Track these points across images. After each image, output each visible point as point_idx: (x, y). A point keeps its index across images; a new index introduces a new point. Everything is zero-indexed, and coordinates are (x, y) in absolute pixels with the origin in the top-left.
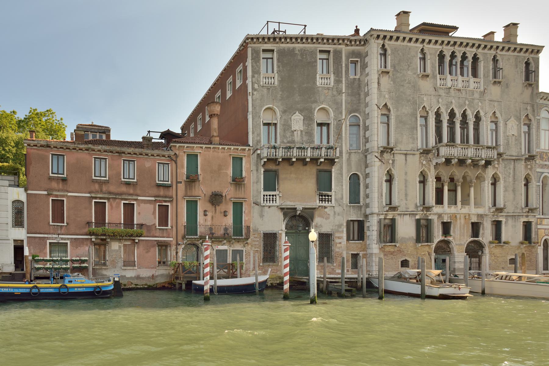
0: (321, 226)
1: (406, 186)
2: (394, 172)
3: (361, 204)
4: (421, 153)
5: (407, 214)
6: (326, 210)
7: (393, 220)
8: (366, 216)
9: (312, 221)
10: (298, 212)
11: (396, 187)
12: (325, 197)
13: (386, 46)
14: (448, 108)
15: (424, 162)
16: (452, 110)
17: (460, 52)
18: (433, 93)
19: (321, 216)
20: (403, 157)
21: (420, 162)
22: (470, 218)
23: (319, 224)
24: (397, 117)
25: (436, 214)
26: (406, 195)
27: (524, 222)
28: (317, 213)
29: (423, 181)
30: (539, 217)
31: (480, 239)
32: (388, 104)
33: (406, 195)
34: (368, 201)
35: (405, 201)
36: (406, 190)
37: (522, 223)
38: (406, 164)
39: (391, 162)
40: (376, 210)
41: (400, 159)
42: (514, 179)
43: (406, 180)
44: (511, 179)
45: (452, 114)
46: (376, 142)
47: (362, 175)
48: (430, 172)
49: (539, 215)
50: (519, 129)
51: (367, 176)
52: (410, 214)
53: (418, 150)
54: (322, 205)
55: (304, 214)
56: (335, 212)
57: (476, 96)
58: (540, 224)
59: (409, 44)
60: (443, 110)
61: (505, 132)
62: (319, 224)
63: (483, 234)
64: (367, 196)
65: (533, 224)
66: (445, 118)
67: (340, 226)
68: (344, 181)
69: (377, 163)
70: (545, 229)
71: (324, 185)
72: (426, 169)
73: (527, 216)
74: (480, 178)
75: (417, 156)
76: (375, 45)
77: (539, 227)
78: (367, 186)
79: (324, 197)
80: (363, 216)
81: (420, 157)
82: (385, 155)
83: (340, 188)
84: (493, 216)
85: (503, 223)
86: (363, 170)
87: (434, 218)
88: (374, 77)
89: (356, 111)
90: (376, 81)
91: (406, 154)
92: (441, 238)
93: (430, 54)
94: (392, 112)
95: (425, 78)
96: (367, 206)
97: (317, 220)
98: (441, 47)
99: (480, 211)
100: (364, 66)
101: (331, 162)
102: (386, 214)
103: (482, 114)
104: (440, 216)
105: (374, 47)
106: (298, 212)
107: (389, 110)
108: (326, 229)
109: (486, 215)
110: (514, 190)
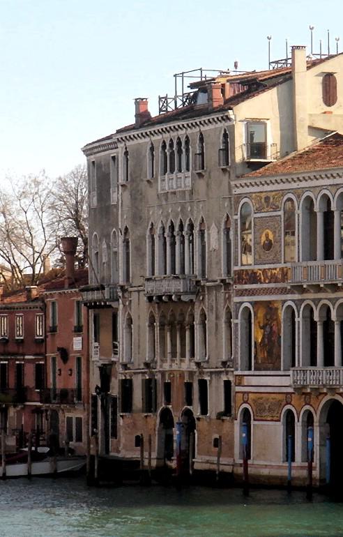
5: (140, 373)
20: (137, 293)
25: (160, 371)
27: (225, 381)
30: (236, 373)
35: (137, 355)
36: (139, 340)
37: (223, 384)
41: (134, 296)
42: (217, 318)
43: (139, 326)
44: (214, 316)
49: (237, 370)
58: (239, 385)
61: (209, 248)
70: (244, 393)
73: (227, 373)
77: (238, 389)
104: (163, 373)
109: (195, 372)
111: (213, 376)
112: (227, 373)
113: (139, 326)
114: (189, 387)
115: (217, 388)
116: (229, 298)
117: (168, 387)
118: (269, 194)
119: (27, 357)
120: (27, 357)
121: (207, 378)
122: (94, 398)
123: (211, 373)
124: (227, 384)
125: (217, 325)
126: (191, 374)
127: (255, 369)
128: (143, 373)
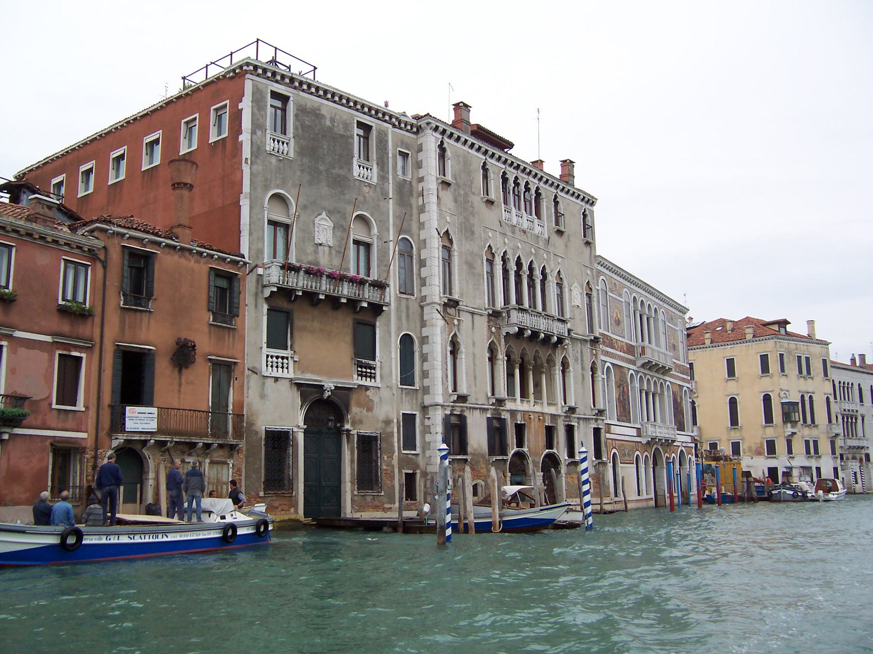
0: (361, 422)
1: (474, 364)
2: (461, 339)
3: (417, 387)
4: (489, 315)
6: (368, 393)
7: (462, 418)
8: (425, 409)
9: (348, 412)
10: (327, 394)
11: (464, 364)
12: (366, 370)
13: (445, 145)
14: (514, 254)
15: (493, 329)
16: (519, 258)
17: (523, 178)
18: (498, 228)
19: (359, 405)
20: (469, 315)
21: (489, 327)
22: (544, 421)
23: (358, 418)
24: (460, 253)
26: (475, 377)
28: (354, 398)
29: (492, 359)
30: (606, 422)
31: (555, 450)
32: (450, 232)
33: (475, 377)
34: (426, 382)
38: (473, 328)
39: (456, 322)
40: (440, 400)
42: (583, 368)
43: (474, 355)
44: (580, 366)
45: (519, 264)
46: (437, 288)
47: (418, 338)
48: (500, 344)
50: (582, 299)
51: (424, 340)
52: (480, 409)
53: (486, 309)
54: (361, 383)
55: (335, 399)
56: (380, 398)
57: (541, 245)
58: (609, 432)
59: (470, 151)
60: (509, 255)
62: (358, 418)
63: (558, 443)
64: (425, 374)
65: (603, 431)
66: (512, 267)
67: (388, 422)
68: (393, 345)
69: (440, 323)
71: (364, 351)
72: (495, 341)
73: (596, 420)
74: (550, 362)
75: (485, 319)
76: (433, 139)
78: (424, 358)
79: (364, 370)
80: (419, 408)
81: (489, 322)
82: (449, 310)
83: (387, 355)
84: (566, 417)
85: (576, 428)
86: (418, 330)
87: (506, 416)
88: (431, 184)
89: (408, 232)
90: (435, 193)
91: (473, 313)
92: (516, 449)
93: (494, 173)
94: (455, 246)
95: (489, 205)
96: (426, 390)
97: (355, 410)
98: (503, 166)
99: (552, 410)
100: (419, 165)
101: (377, 309)
102: (453, 407)
103: (548, 271)
104: (513, 413)
105: (431, 141)
106: (327, 394)
107: (451, 241)
108: (366, 430)
110: (583, 383)
111: (581, 422)
112: (596, 420)
113: (474, 355)
114: (550, 431)
115: (586, 434)
116: (596, 355)
117: (520, 429)
118: (617, 283)
119: (18, 334)
120: (18, 334)
121: (576, 424)
122: (278, 440)
123: (579, 418)
124: (597, 431)
125: (583, 376)
126: (554, 417)
127: (618, 420)
128: (485, 410)
